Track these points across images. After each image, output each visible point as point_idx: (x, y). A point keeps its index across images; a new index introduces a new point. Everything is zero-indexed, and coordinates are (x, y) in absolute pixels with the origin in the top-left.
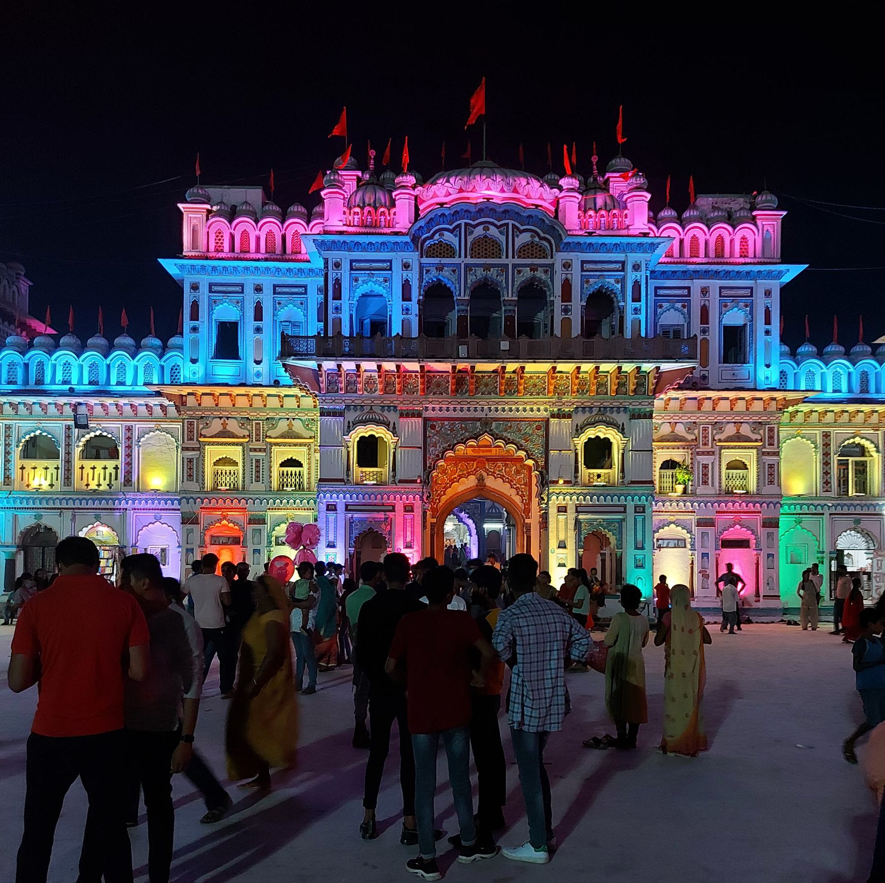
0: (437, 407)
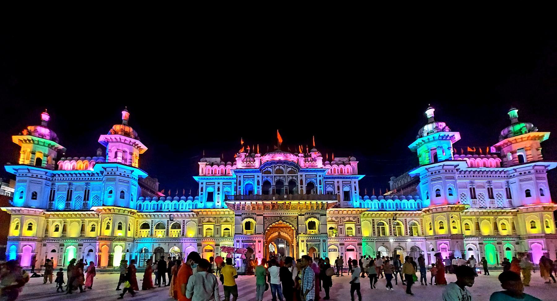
0: (267, 213)
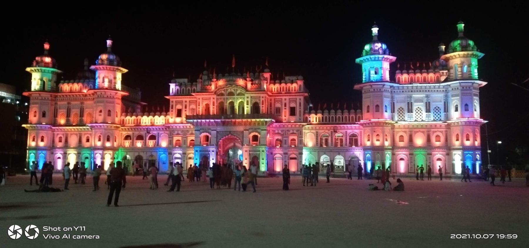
0: (219, 129)
